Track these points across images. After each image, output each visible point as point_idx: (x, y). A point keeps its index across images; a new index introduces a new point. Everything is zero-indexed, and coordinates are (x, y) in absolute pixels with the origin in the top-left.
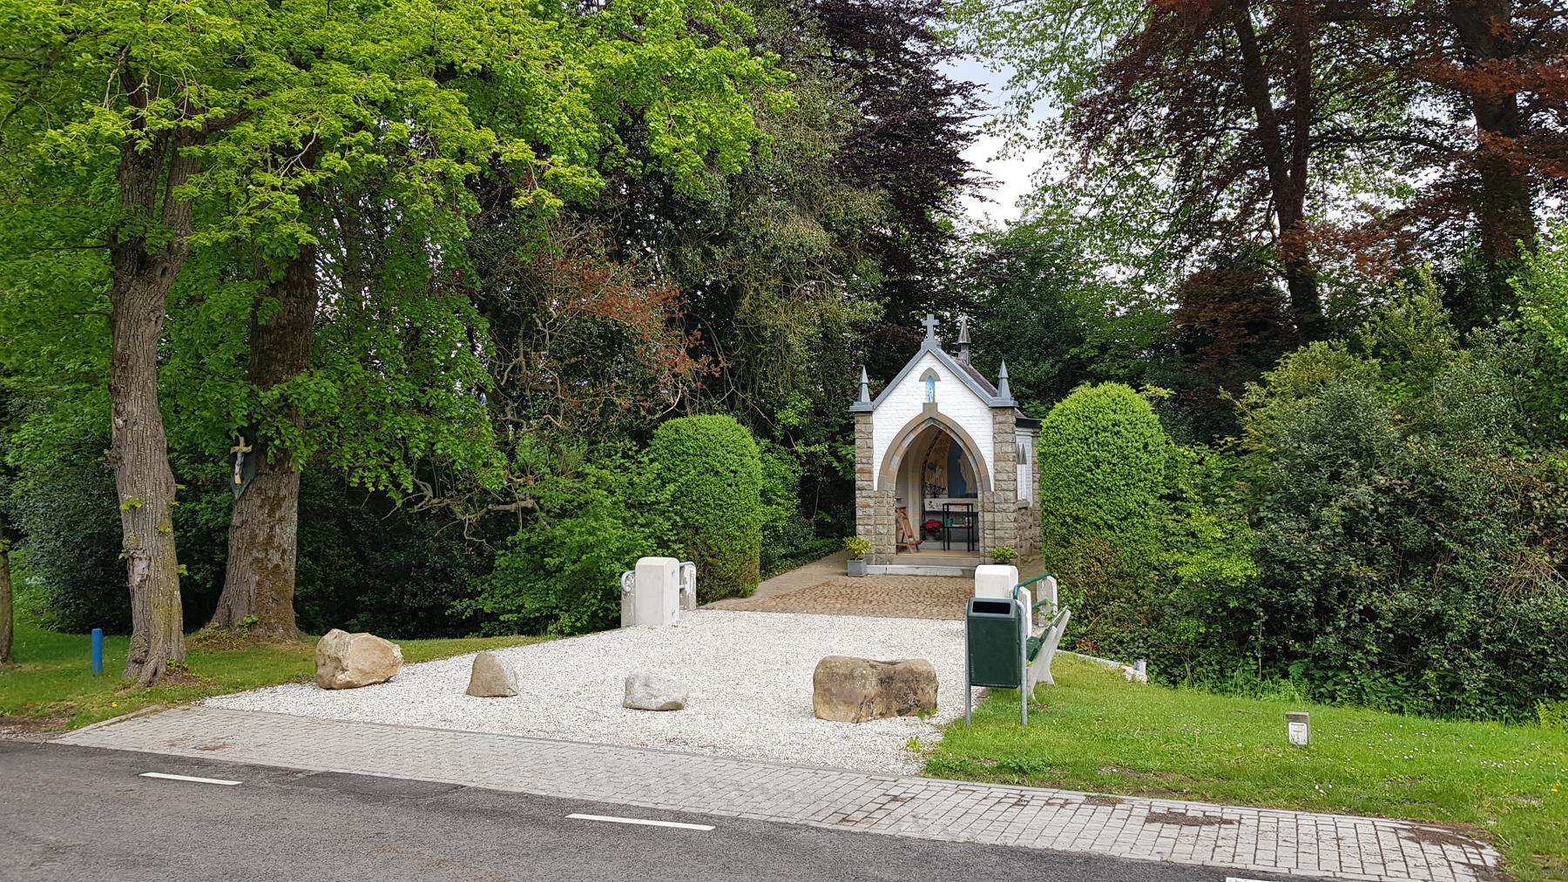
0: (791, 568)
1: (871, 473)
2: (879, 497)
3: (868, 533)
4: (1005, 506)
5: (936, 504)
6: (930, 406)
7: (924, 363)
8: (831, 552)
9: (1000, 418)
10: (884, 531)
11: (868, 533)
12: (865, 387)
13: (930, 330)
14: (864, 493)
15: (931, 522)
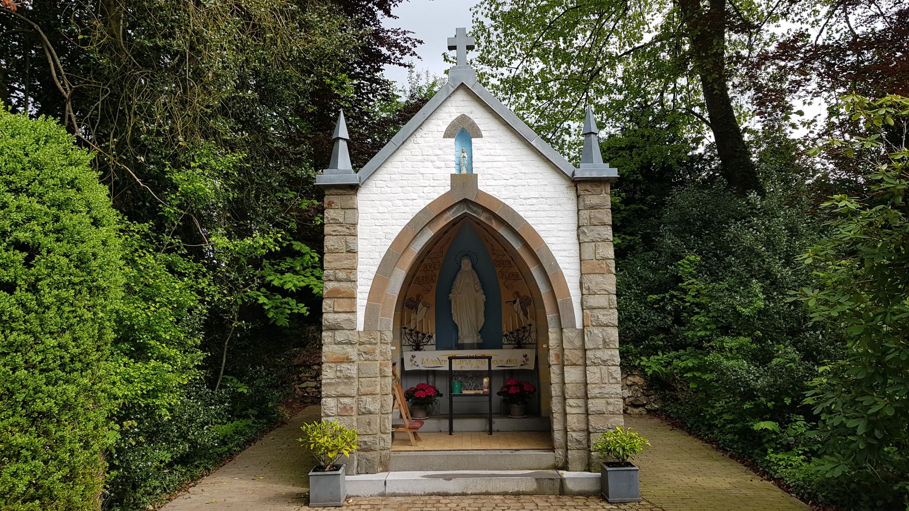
0: (182, 487)
1: (352, 297)
2: (366, 344)
3: (344, 412)
4: (605, 354)
5: (431, 358)
6: (464, 180)
8: (249, 442)
10: (374, 406)
11: (344, 412)
12: (343, 147)
14: (340, 336)
15: (420, 388)
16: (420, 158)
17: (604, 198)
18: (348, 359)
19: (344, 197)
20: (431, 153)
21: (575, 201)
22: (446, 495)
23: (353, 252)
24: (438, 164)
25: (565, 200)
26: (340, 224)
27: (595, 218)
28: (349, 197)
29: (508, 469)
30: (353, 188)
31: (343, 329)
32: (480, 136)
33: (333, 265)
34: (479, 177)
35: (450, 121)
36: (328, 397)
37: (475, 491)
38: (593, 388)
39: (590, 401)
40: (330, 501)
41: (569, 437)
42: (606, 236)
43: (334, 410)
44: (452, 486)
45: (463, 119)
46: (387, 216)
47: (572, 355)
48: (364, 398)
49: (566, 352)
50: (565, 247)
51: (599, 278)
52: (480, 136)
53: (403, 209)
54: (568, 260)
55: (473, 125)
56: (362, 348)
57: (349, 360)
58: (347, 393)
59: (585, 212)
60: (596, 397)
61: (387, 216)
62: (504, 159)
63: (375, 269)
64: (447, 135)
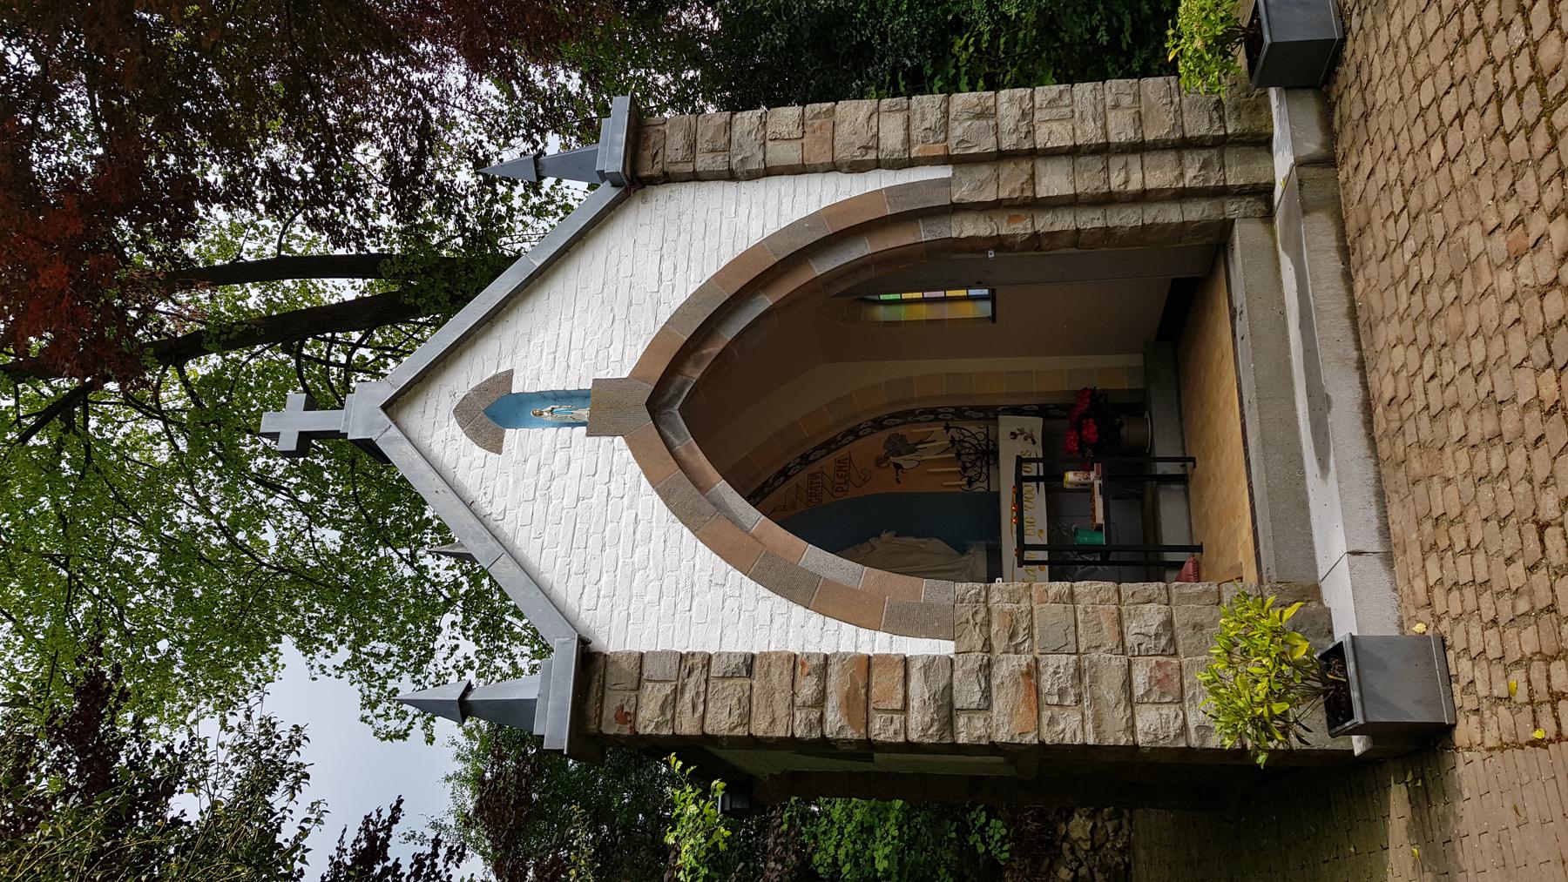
1: (868, 663)
14: (968, 694)
16: (539, 505)
18: (1028, 674)
19: (611, 680)
20: (532, 481)
21: (676, 187)
22: (1368, 407)
23: (750, 662)
24: (558, 464)
25: (672, 205)
26: (678, 692)
27: (713, 140)
28: (611, 669)
29: (1283, 313)
30: (589, 661)
31: (950, 686)
32: (509, 375)
33: (781, 711)
34: (602, 375)
35: (464, 440)
36: (1131, 728)
37: (1351, 343)
38: (1084, 133)
39: (1113, 139)
40: (1430, 663)
41: (1198, 183)
42: (755, 119)
43: (1169, 711)
44: (1344, 395)
45: (464, 413)
46: (669, 582)
47: (1010, 182)
48: (1130, 640)
49: (1004, 194)
50: (772, 203)
51: (844, 130)
52: (509, 375)
53: (656, 543)
54: (801, 198)
55: (480, 390)
56: (999, 644)
57: (1032, 673)
58: (1118, 680)
59: (699, 160)
60: (1104, 126)
61: (669, 582)
62: (566, 326)
63: (798, 610)
64: (495, 446)
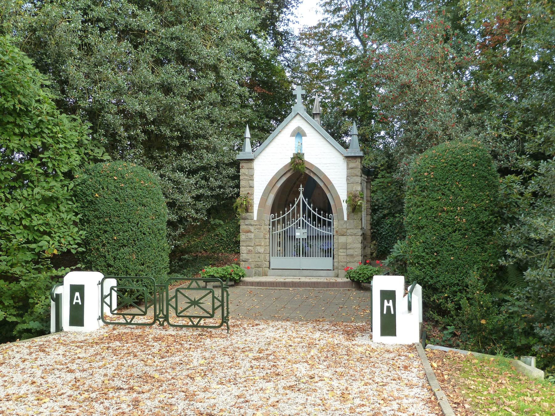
7: (295, 123)
9: (352, 165)
10: (261, 250)
11: (249, 252)
13: (299, 97)
14: (247, 222)
17: (357, 164)
23: (252, 187)
43: (245, 251)
45: (299, 128)
48: (257, 247)
55: (303, 131)
64: (292, 135)
